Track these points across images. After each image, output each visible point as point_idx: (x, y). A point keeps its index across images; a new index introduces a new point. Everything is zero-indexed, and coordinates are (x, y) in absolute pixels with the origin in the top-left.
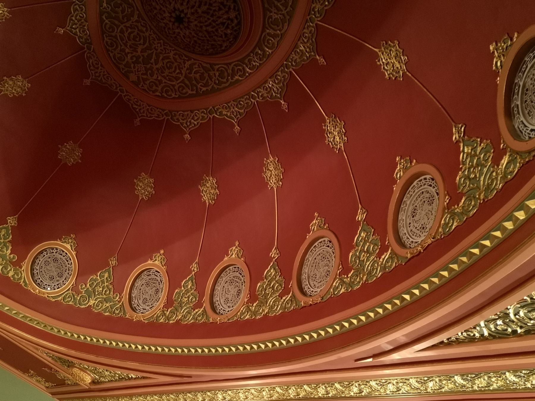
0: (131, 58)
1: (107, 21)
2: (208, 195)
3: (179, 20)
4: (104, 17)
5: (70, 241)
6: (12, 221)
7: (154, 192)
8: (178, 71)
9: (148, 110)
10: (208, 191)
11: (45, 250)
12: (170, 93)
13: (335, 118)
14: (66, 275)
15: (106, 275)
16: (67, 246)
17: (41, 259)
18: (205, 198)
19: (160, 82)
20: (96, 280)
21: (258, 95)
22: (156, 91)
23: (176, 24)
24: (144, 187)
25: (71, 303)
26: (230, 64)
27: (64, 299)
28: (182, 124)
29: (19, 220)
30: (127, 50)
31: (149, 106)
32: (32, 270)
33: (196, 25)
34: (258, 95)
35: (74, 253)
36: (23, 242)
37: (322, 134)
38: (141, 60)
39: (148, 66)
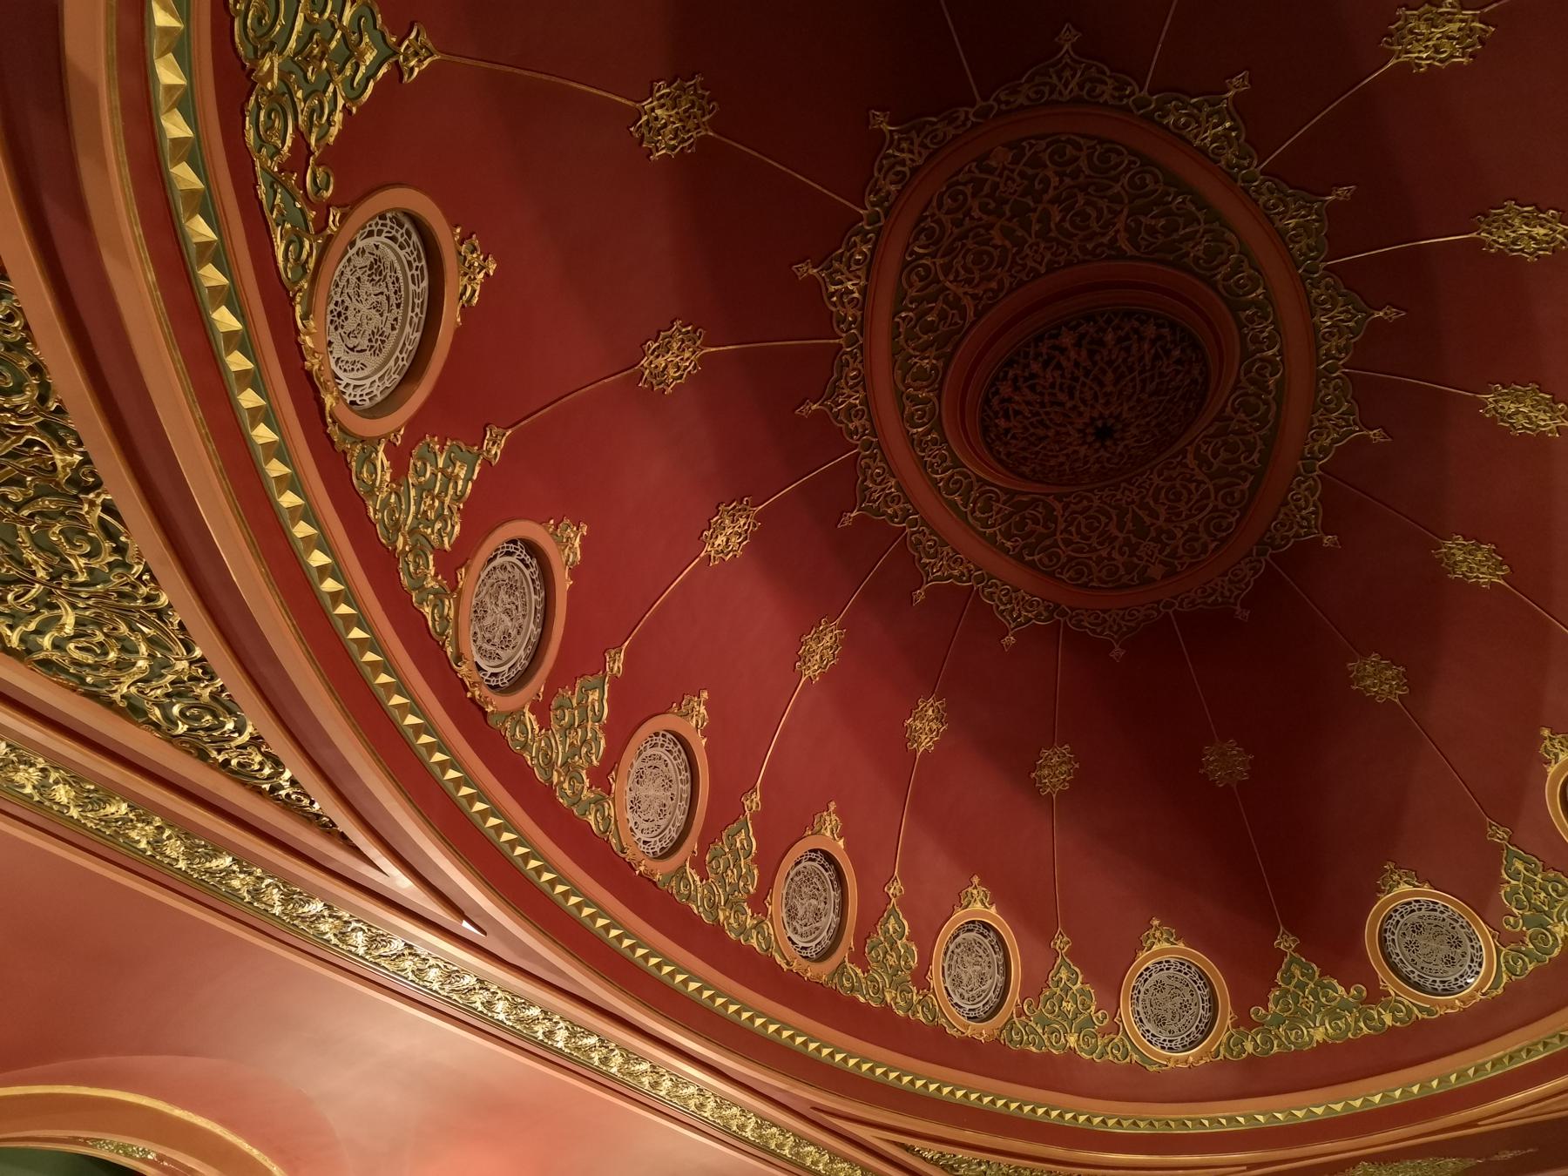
0: (1122, 554)
1: (1036, 558)
2: (1484, 569)
3: (1104, 434)
4: (1028, 558)
5: (1396, 877)
6: (1286, 943)
7: (1401, 669)
8: (1193, 486)
9: (1231, 581)
10: (1475, 565)
11: (1383, 931)
12: (1225, 525)
13: (1486, 216)
14: (1462, 934)
15: (1519, 865)
16: (1403, 890)
17: (1397, 951)
18: (1485, 579)
19: (1194, 528)
20: (1515, 891)
21: (1333, 357)
22: (1205, 545)
23: (1108, 443)
24: (1379, 679)
25: (1530, 967)
26: (1238, 381)
27: (1511, 971)
28: (1297, 535)
29: (1292, 930)
30: (1104, 554)
31: (1225, 574)
32: (1407, 980)
33: (1131, 409)
34: (1333, 357)
35: (1426, 888)
36: (1338, 952)
37: (1507, 263)
38: (1134, 540)
39: (1153, 534)
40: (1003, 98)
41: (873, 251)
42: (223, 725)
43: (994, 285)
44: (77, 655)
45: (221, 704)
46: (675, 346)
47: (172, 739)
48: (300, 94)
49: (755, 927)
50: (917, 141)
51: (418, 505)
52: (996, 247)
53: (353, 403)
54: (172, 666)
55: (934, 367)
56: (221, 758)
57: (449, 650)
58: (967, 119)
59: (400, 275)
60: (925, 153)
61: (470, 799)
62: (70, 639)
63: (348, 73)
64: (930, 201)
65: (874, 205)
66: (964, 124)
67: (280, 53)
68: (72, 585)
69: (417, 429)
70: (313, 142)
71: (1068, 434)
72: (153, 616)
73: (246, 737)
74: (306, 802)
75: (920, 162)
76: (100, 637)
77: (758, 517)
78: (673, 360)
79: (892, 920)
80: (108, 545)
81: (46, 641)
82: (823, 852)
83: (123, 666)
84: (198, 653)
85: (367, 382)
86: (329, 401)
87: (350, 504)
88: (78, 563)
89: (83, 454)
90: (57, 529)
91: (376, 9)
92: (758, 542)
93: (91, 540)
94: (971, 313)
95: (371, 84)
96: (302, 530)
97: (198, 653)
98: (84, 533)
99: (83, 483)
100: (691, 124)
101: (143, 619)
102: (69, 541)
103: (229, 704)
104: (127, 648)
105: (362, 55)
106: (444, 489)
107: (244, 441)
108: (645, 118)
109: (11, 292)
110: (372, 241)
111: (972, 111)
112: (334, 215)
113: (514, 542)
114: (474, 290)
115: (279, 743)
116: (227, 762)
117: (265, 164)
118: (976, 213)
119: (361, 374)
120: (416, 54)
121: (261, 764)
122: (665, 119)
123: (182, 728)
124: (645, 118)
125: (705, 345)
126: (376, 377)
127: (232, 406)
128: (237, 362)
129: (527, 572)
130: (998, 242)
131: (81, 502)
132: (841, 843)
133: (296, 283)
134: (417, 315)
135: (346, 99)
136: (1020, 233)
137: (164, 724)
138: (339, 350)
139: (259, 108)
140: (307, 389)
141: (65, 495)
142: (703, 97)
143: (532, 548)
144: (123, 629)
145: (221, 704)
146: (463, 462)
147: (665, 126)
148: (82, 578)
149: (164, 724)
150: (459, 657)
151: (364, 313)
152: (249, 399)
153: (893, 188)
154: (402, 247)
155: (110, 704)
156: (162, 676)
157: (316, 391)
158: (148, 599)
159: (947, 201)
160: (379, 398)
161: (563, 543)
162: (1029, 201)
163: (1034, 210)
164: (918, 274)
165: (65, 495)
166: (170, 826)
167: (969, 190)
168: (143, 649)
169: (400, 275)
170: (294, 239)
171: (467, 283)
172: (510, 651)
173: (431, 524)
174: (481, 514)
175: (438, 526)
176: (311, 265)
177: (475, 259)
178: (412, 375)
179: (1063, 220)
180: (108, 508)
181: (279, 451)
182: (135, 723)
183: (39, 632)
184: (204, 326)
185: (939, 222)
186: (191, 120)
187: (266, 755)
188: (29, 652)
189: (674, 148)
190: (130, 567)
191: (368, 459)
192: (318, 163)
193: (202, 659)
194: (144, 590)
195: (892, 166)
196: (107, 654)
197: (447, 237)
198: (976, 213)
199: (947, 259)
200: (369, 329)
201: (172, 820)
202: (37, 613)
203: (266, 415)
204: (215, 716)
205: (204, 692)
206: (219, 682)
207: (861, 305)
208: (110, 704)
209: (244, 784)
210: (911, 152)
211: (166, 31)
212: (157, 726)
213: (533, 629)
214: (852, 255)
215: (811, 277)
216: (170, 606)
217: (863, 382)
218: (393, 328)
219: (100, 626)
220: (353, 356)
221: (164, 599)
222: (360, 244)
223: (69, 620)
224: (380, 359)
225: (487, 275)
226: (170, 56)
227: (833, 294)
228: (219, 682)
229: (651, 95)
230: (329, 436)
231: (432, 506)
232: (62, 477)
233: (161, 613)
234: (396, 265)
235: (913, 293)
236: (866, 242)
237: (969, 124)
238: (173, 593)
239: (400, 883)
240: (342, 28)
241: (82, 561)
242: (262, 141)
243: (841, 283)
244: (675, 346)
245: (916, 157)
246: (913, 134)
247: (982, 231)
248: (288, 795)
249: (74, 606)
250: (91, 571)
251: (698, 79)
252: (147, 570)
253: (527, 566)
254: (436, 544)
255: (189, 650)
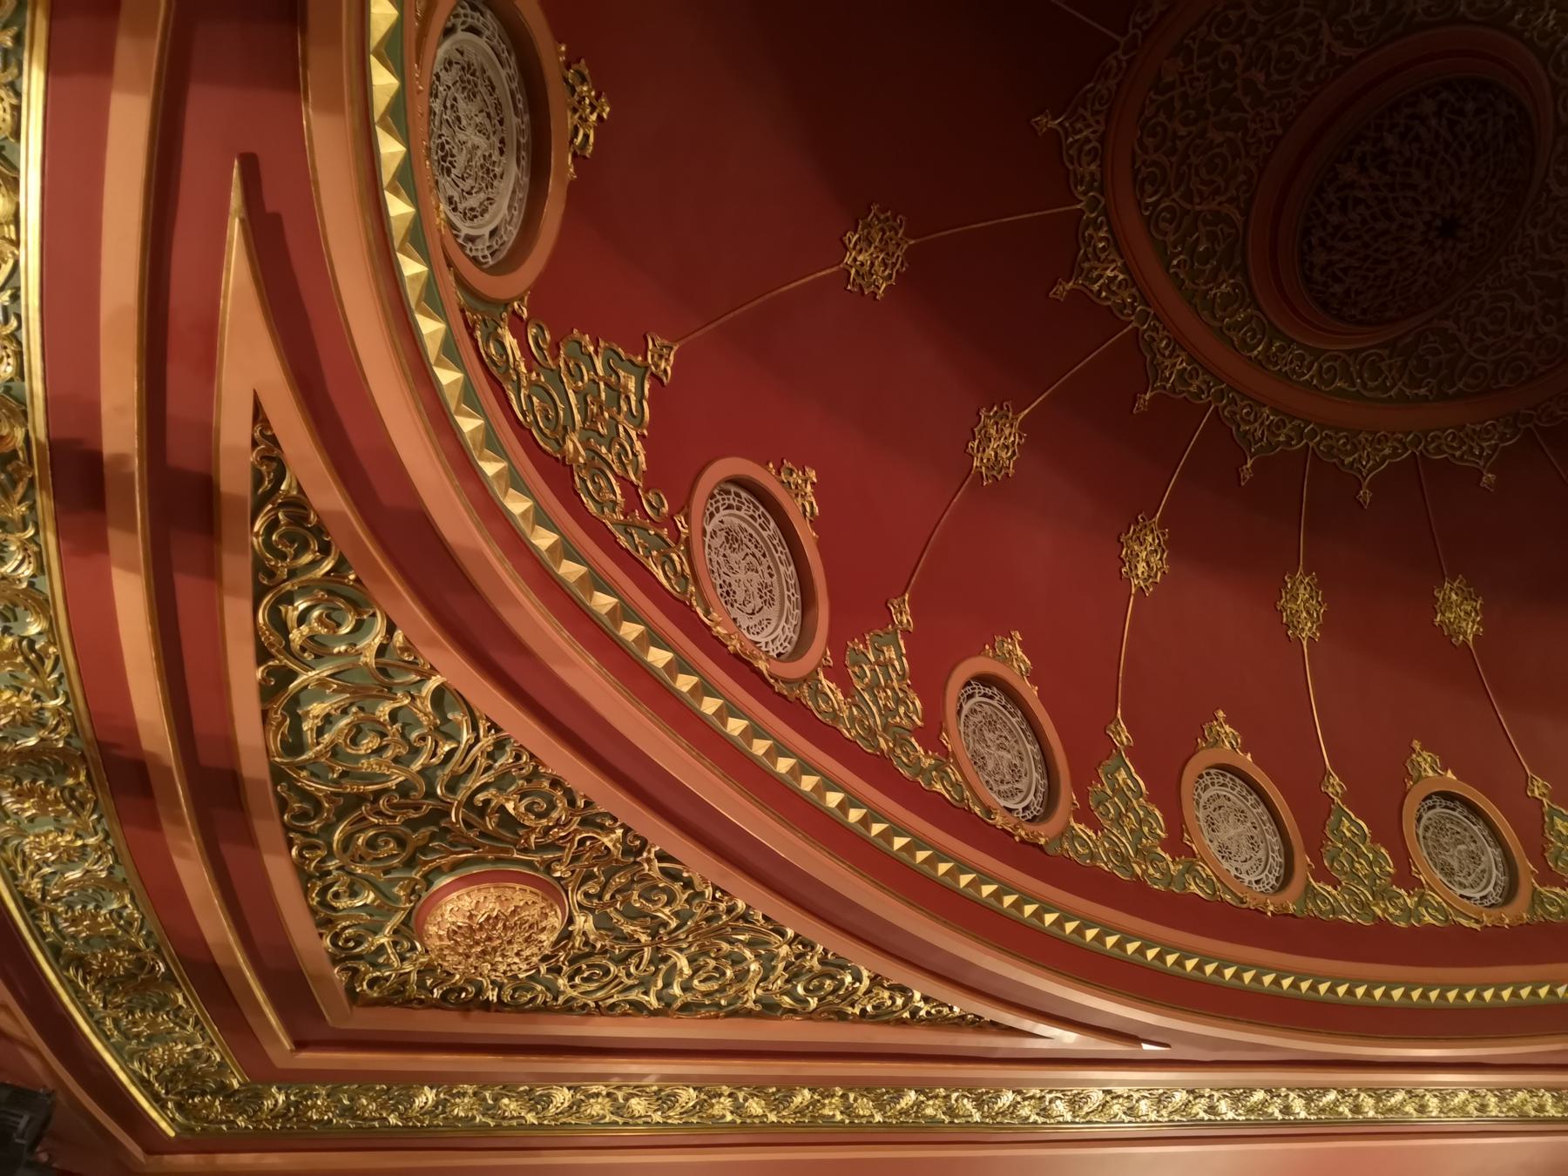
4: (1451, 392)
30: (1530, 335)
40: (1139, 19)
41: (1110, 231)
42: (842, 982)
43: (1242, 178)
44: (704, 987)
45: (832, 966)
46: (993, 432)
47: (810, 1016)
48: (604, 450)
49: (1419, 904)
50: (1088, 114)
51: (876, 703)
52: (1220, 145)
53: (779, 655)
54: (777, 955)
55: (1234, 286)
56: (857, 1011)
57: (977, 810)
58: (1119, 62)
59: (751, 531)
60: (1101, 118)
61: (1079, 931)
62: (692, 977)
63: (625, 408)
64: (1134, 152)
65: (1085, 193)
66: (1119, 67)
67: (574, 430)
68: (669, 933)
69: (837, 642)
70: (633, 478)
71: (1412, 254)
72: (741, 923)
73: (866, 982)
74: (946, 1010)
75: (1102, 128)
76: (712, 963)
77: (1162, 525)
78: (998, 445)
79: (1558, 821)
80: (677, 886)
81: (676, 990)
82: (1436, 794)
83: (742, 976)
84: (790, 933)
85: (779, 630)
86: (762, 665)
87: (824, 734)
88: (664, 913)
89: (622, 826)
90: (635, 897)
91: (615, 346)
92: (1175, 548)
93: (663, 890)
94: (1237, 217)
95: (645, 404)
96: (808, 783)
97: (790, 933)
98: (655, 887)
99: (634, 848)
100: (891, 248)
101: (736, 930)
102: (648, 900)
103: (840, 962)
104: (737, 960)
105: (626, 387)
106: (888, 677)
107: (725, 740)
108: (853, 271)
109: (508, 738)
110: (717, 517)
111: (1119, 53)
112: (680, 520)
113: (968, 684)
114: (811, 503)
115: (896, 973)
116: (863, 1011)
117: (612, 519)
118: (1183, 131)
119: (771, 628)
120: (661, 357)
121: (891, 998)
122: (869, 261)
123: (813, 1002)
124: (853, 271)
125: (1016, 413)
126: (783, 623)
127: (700, 718)
128: (684, 683)
129: (995, 703)
130: (1220, 139)
131: (640, 864)
132: (1450, 774)
133: (685, 592)
134: (782, 553)
135: (636, 427)
136: (1235, 116)
137: (798, 1007)
138: (744, 622)
139: (584, 481)
140: (741, 666)
141: (626, 866)
142: (887, 219)
143: (985, 680)
144: (725, 946)
145: (832, 966)
146: (887, 645)
147: (872, 264)
148: (673, 924)
149: (798, 1007)
150: (989, 811)
151: (744, 580)
152: (710, 706)
153: (1093, 167)
154: (739, 509)
155: (749, 1014)
156: (774, 968)
157: (749, 664)
158: (730, 910)
159: (1149, 141)
160: (795, 638)
161: (1007, 660)
162: (1224, 84)
163: (1235, 89)
164: (1165, 220)
165: (626, 866)
166: (851, 1090)
167: (1162, 118)
168: (748, 954)
169: (751, 531)
170: (665, 560)
171: (803, 504)
172: (1025, 780)
173: (895, 712)
174: (928, 677)
175: (902, 710)
176: (687, 571)
177: (797, 478)
178: (807, 603)
179: (1268, 75)
180: (661, 857)
181: (755, 731)
182: (779, 1018)
183: (667, 985)
184: (646, 671)
185: (1154, 163)
186: (552, 527)
187: (891, 988)
188: (668, 1005)
189: (890, 276)
190: (702, 894)
191: (817, 692)
192: (646, 491)
193: (797, 936)
194: (722, 906)
195: (1080, 151)
196: (724, 974)
197: (765, 477)
198: (1183, 131)
199: (1182, 188)
200: (754, 589)
201: (849, 1084)
202: (657, 970)
203: (730, 710)
204: (833, 978)
205: (813, 962)
206: (820, 948)
207: (1132, 281)
208: (749, 1014)
209: (887, 1022)
210: (1089, 126)
211: (498, 475)
212: (793, 1011)
213: (1031, 748)
214: (1095, 247)
215: (1072, 290)
216: (748, 907)
217: (1178, 343)
218: (771, 576)
219: (707, 954)
220: (757, 618)
221: (741, 905)
222: (709, 529)
223: (683, 963)
224: (777, 606)
225: (813, 484)
226: (511, 491)
227: (1100, 292)
228: (820, 948)
229: (847, 249)
230: (779, 694)
231: (887, 698)
232: (617, 853)
233: (744, 917)
234: (744, 525)
235: (1171, 238)
236: (1099, 228)
237: (1124, 65)
238: (746, 896)
239: (1067, 1039)
240: (601, 378)
241: (667, 910)
242: (600, 504)
243: (1100, 276)
244: (993, 432)
245: (1096, 127)
246: (1081, 110)
247: (1198, 141)
248: (928, 1013)
249: (680, 950)
250: (676, 914)
251: (875, 208)
252: (716, 888)
253: (991, 698)
254: (910, 727)
255: (783, 935)
